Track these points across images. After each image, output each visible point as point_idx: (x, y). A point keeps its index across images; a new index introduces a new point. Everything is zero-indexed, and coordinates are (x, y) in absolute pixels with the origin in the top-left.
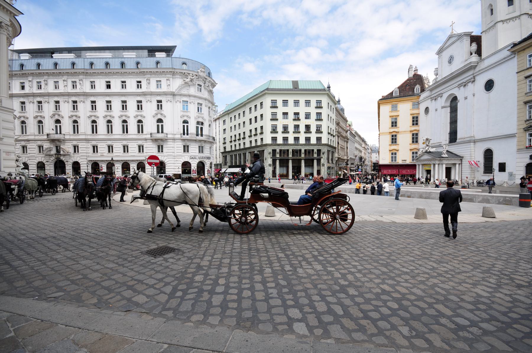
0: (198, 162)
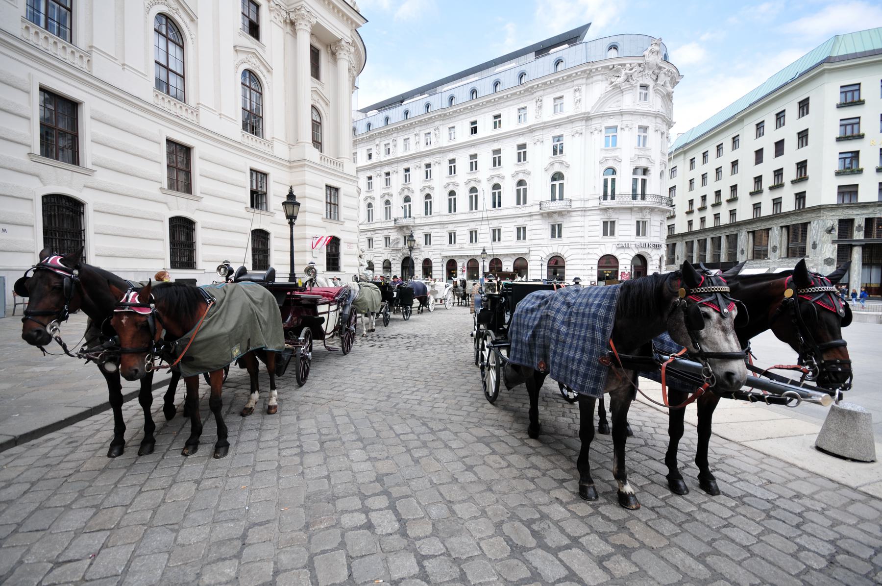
0: (634, 255)
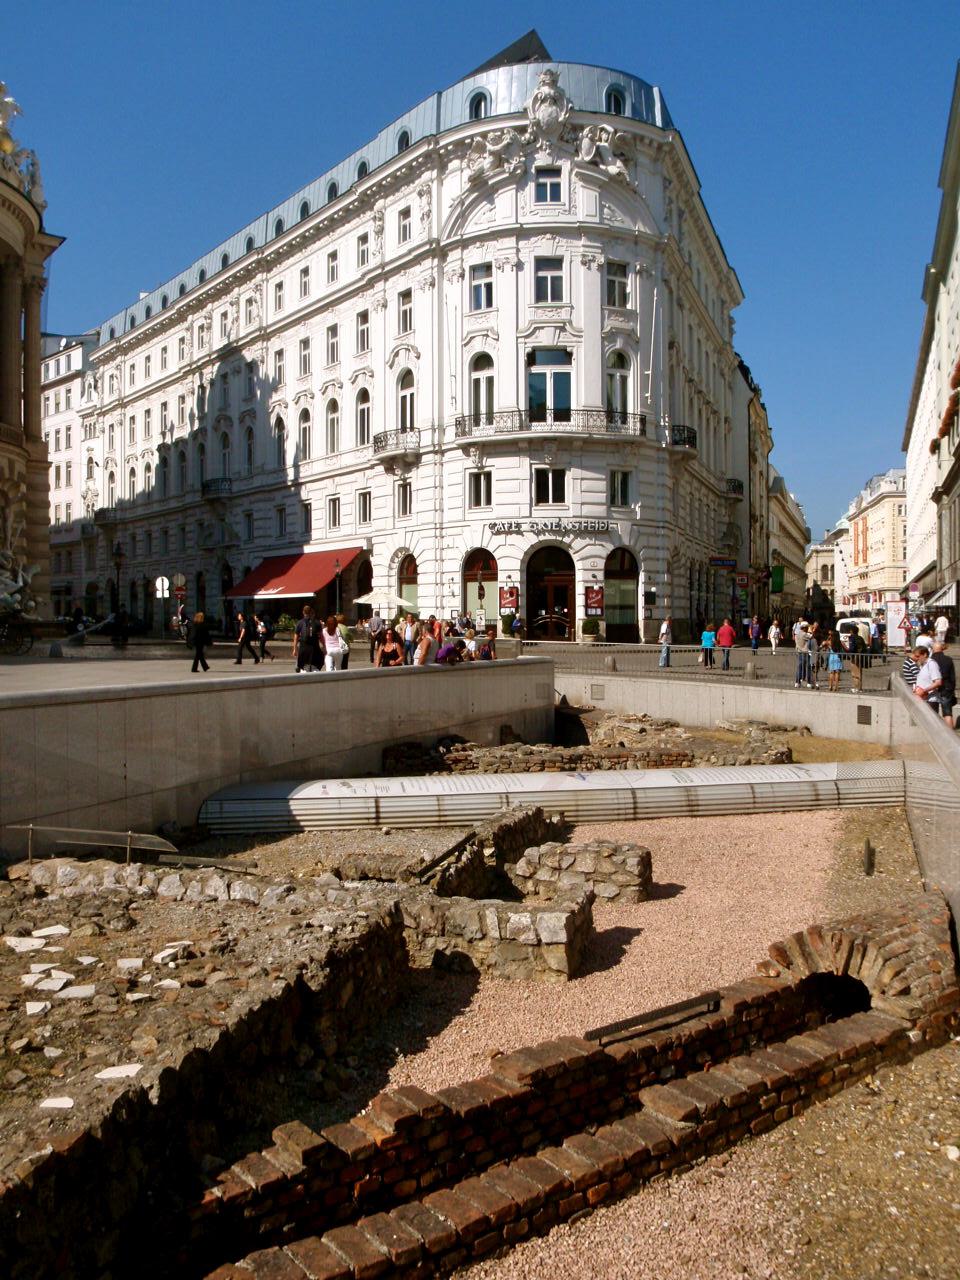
0: (526, 547)
